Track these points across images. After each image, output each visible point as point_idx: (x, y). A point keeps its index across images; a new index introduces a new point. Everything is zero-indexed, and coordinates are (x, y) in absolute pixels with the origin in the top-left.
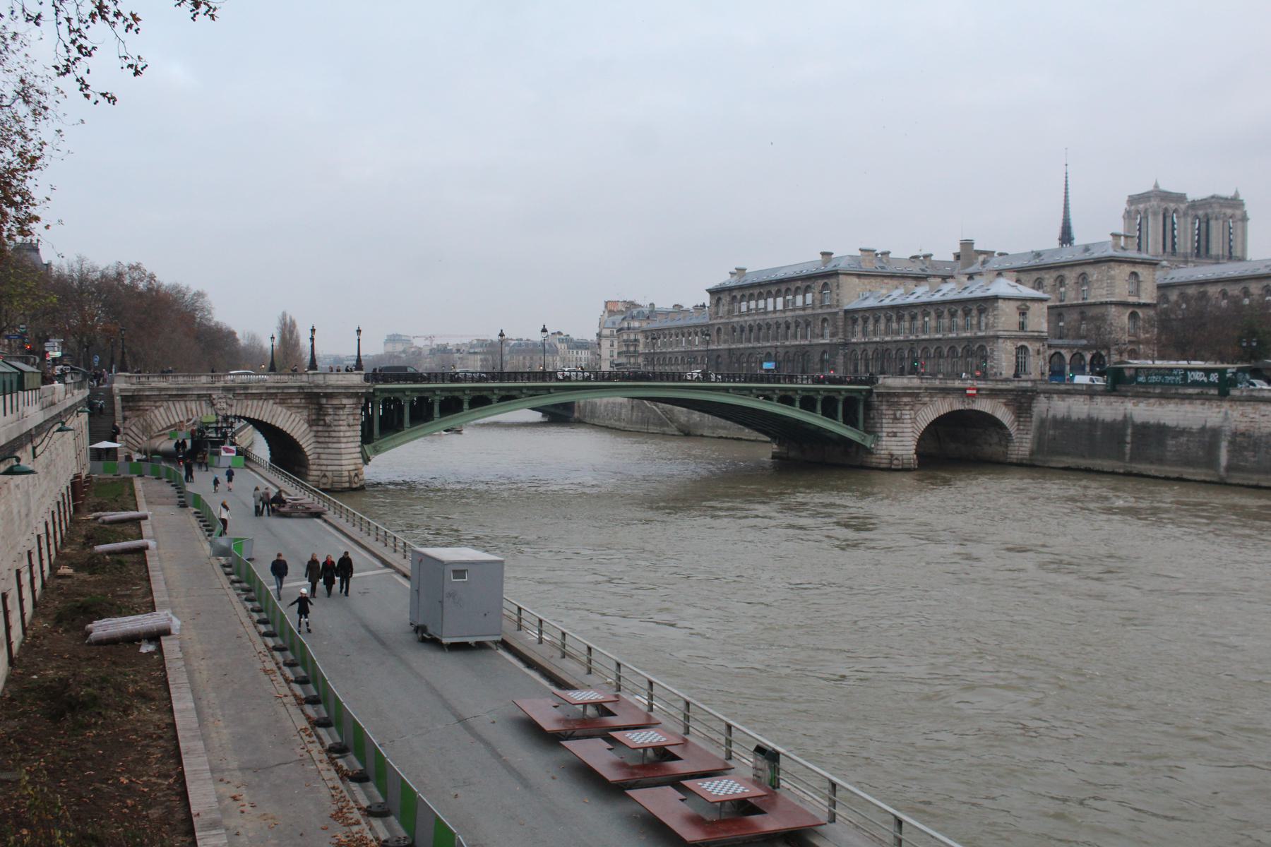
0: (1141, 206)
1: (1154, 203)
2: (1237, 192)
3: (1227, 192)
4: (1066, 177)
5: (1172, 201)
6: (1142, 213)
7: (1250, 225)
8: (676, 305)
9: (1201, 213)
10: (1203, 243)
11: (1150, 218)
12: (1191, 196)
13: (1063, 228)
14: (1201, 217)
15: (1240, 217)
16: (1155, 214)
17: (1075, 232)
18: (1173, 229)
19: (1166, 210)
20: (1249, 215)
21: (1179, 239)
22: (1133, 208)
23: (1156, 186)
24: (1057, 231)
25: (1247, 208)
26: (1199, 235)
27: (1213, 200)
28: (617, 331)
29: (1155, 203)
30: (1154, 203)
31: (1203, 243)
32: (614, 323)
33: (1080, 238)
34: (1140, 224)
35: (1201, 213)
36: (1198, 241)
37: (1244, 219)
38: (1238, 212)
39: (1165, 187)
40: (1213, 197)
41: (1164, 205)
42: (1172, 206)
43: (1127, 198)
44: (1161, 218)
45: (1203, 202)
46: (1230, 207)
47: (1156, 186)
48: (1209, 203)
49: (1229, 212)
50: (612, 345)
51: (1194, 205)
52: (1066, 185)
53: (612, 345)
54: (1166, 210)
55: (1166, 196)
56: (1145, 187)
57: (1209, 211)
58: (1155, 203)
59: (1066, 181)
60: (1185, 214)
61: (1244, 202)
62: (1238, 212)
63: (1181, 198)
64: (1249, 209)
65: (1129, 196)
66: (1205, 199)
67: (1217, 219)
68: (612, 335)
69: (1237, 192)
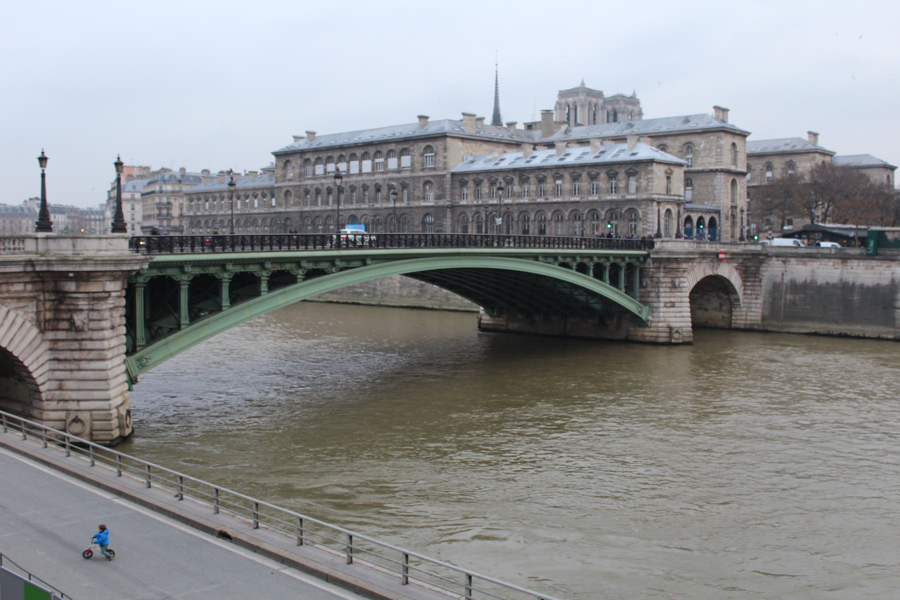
1: (582, 97)
2: (634, 92)
3: (628, 93)
5: (594, 97)
6: (571, 106)
11: (579, 109)
12: (607, 94)
13: (494, 116)
16: (582, 106)
19: (590, 103)
20: (644, 111)
22: (563, 100)
23: (583, 84)
25: (641, 106)
28: (143, 195)
29: (583, 97)
30: (582, 97)
32: (134, 187)
34: (568, 114)
35: (610, 108)
38: (636, 109)
39: (589, 85)
40: (618, 96)
41: (589, 99)
42: (594, 100)
43: (558, 93)
44: (587, 109)
47: (583, 84)
48: (616, 100)
49: (630, 107)
50: (133, 209)
51: (608, 101)
53: (133, 209)
55: (590, 93)
56: (572, 84)
57: (617, 106)
58: (583, 97)
60: (603, 108)
63: (599, 94)
64: (642, 105)
65: (560, 91)
66: (613, 97)
67: (623, 113)
68: (133, 199)
69: (634, 92)
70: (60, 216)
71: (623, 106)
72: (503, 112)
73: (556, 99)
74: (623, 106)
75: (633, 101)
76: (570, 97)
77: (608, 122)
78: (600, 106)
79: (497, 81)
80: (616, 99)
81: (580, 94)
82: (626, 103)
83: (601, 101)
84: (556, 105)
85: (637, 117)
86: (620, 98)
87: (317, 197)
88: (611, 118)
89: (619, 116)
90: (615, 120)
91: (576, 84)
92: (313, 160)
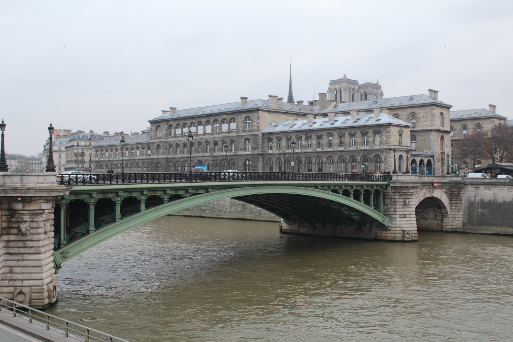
0: (337, 86)
1: (345, 84)
2: (378, 81)
3: (374, 82)
4: (290, 71)
5: (352, 84)
8: (106, 132)
11: (342, 92)
12: (361, 82)
15: (380, 94)
16: (345, 90)
19: (350, 88)
20: (384, 93)
22: (333, 87)
23: (345, 76)
27: (369, 85)
28: (66, 148)
29: (345, 85)
32: (61, 143)
34: (336, 95)
35: (362, 91)
38: (379, 91)
39: (349, 77)
41: (349, 86)
42: (352, 86)
43: (329, 82)
44: (348, 92)
45: (363, 85)
46: (376, 88)
47: (345, 76)
49: (375, 91)
50: (60, 157)
52: (290, 75)
53: (60, 157)
55: (350, 82)
57: (367, 90)
58: (345, 85)
59: (290, 73)
60: (358, 91)
61: (381, 86)
62: (379, 91)
63: (355, 83)
66: (364, 84)
67: (370, 94)
68: (60, 150)
69: (378, 81)
70: (13, 161)
71: (371, 90)
72: (294, 95)
73: (328, 86)
74: (371, 90)
75: (377, 86)
76: (337, 85)
77: (361, 100)
78: (356, 90)
79: (290, 75)
80: (366, 86)
81: (343, 83)
82: (372, 88)
83: (357, 87)
84: (328, 90)
85: (380, 97)
86: (369, 85)
87: (177, 149)
88: (363, 97)
89: (369, 96)
90: (366, 99)
91: (340, 76)
92: (174, 125)
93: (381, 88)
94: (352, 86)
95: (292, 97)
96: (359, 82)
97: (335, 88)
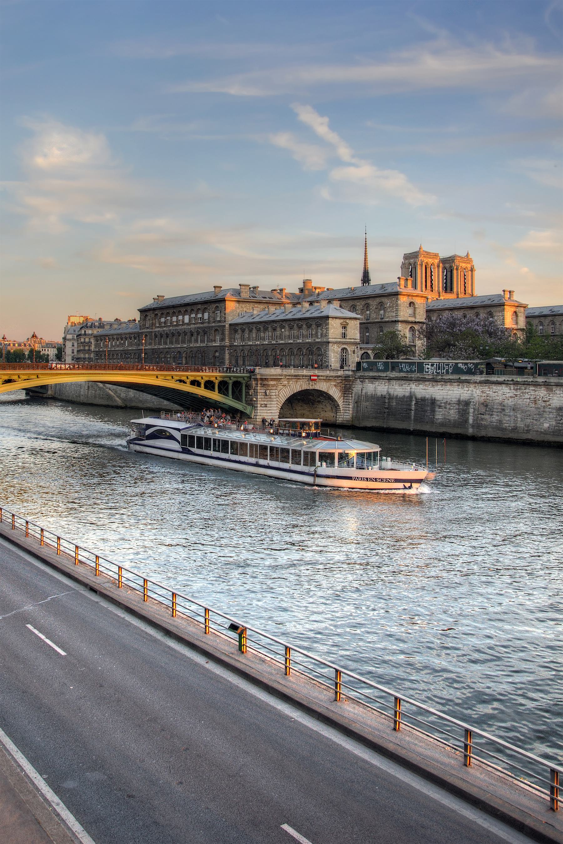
2: (468, 253)
5: (430, 258)
6: (412, 265)
7: (476, 273)
8: (117, 319)
9: (447, 266)
10: (449, 284)
14: (447, 268)
15: (470, 269)
17: (372, 276)
18: (431, 275)
21: (435, 281)
22: (407, 261)
24: (360, 275)
26: (446, 279)
28: (77, 336)
31: (449, 284)
32: (75, 331)
33: (376, 279)
34: (411, 272)
35: (447, 266)
36: (446, 283)
37: (472, 270)
50: (73, 346)
53: (73, 346)
54: (427, 263)
59: (366, 244)
68: (73, 339)
69: (468, 253)
83: (436, 261)
92: (189, 311)
93: (472, 261)
94: (430, 260)
95: (368, 273)
96: (440, 255)
97: (410, 263)
